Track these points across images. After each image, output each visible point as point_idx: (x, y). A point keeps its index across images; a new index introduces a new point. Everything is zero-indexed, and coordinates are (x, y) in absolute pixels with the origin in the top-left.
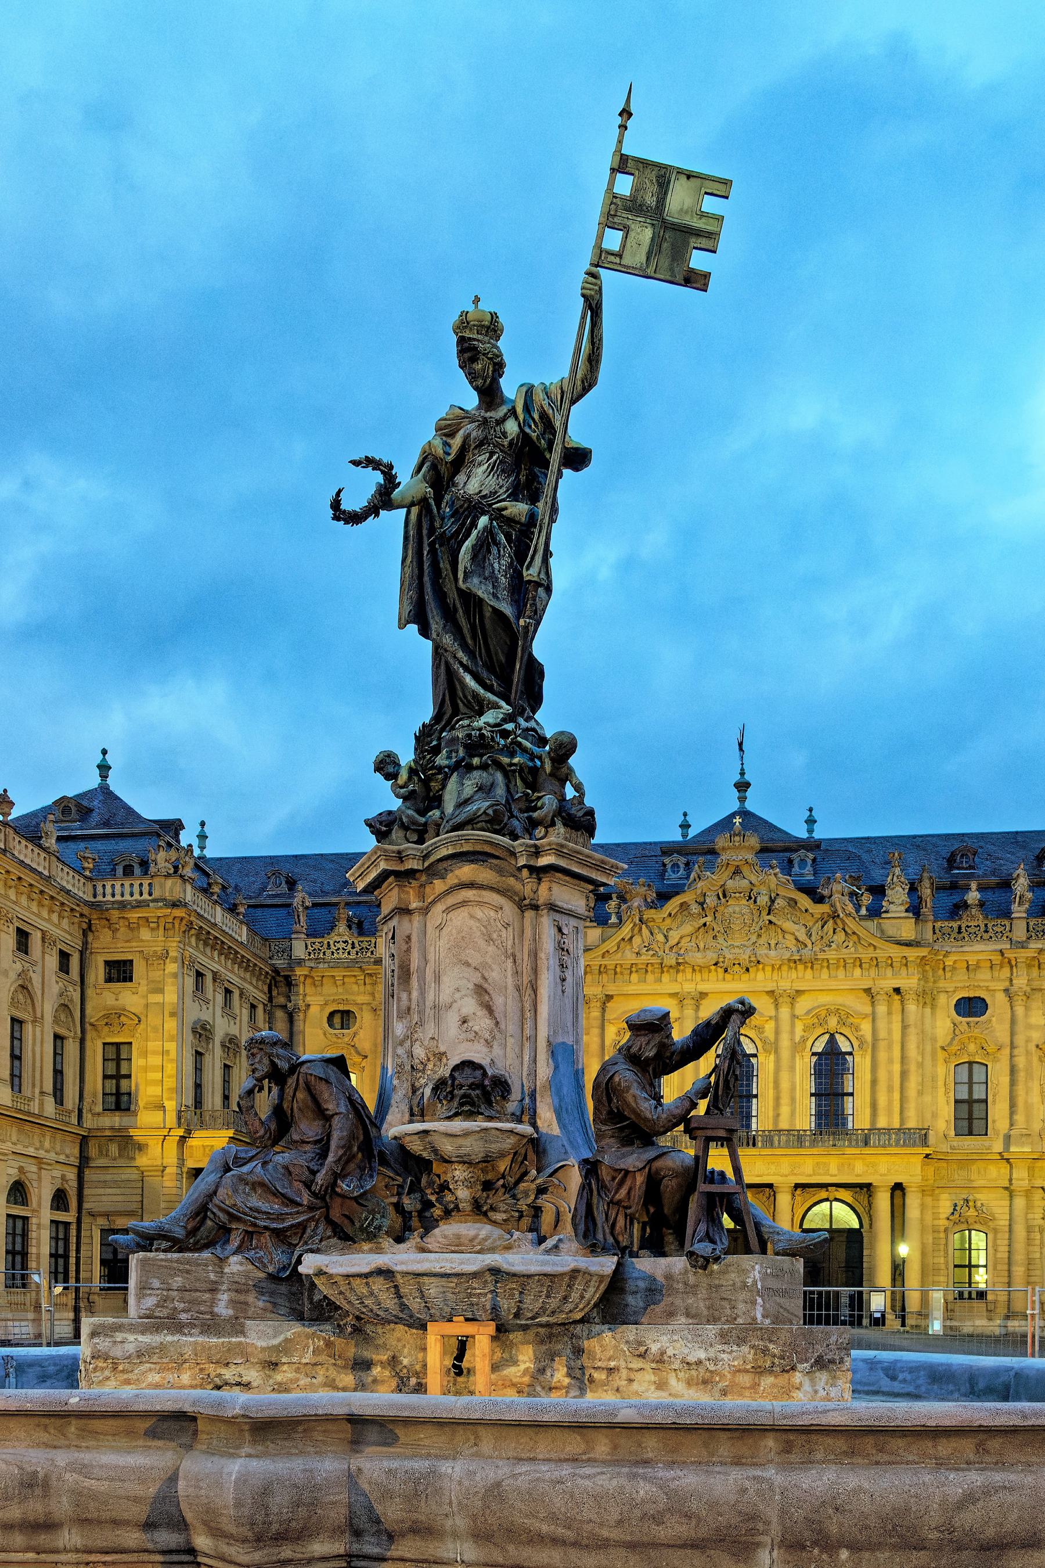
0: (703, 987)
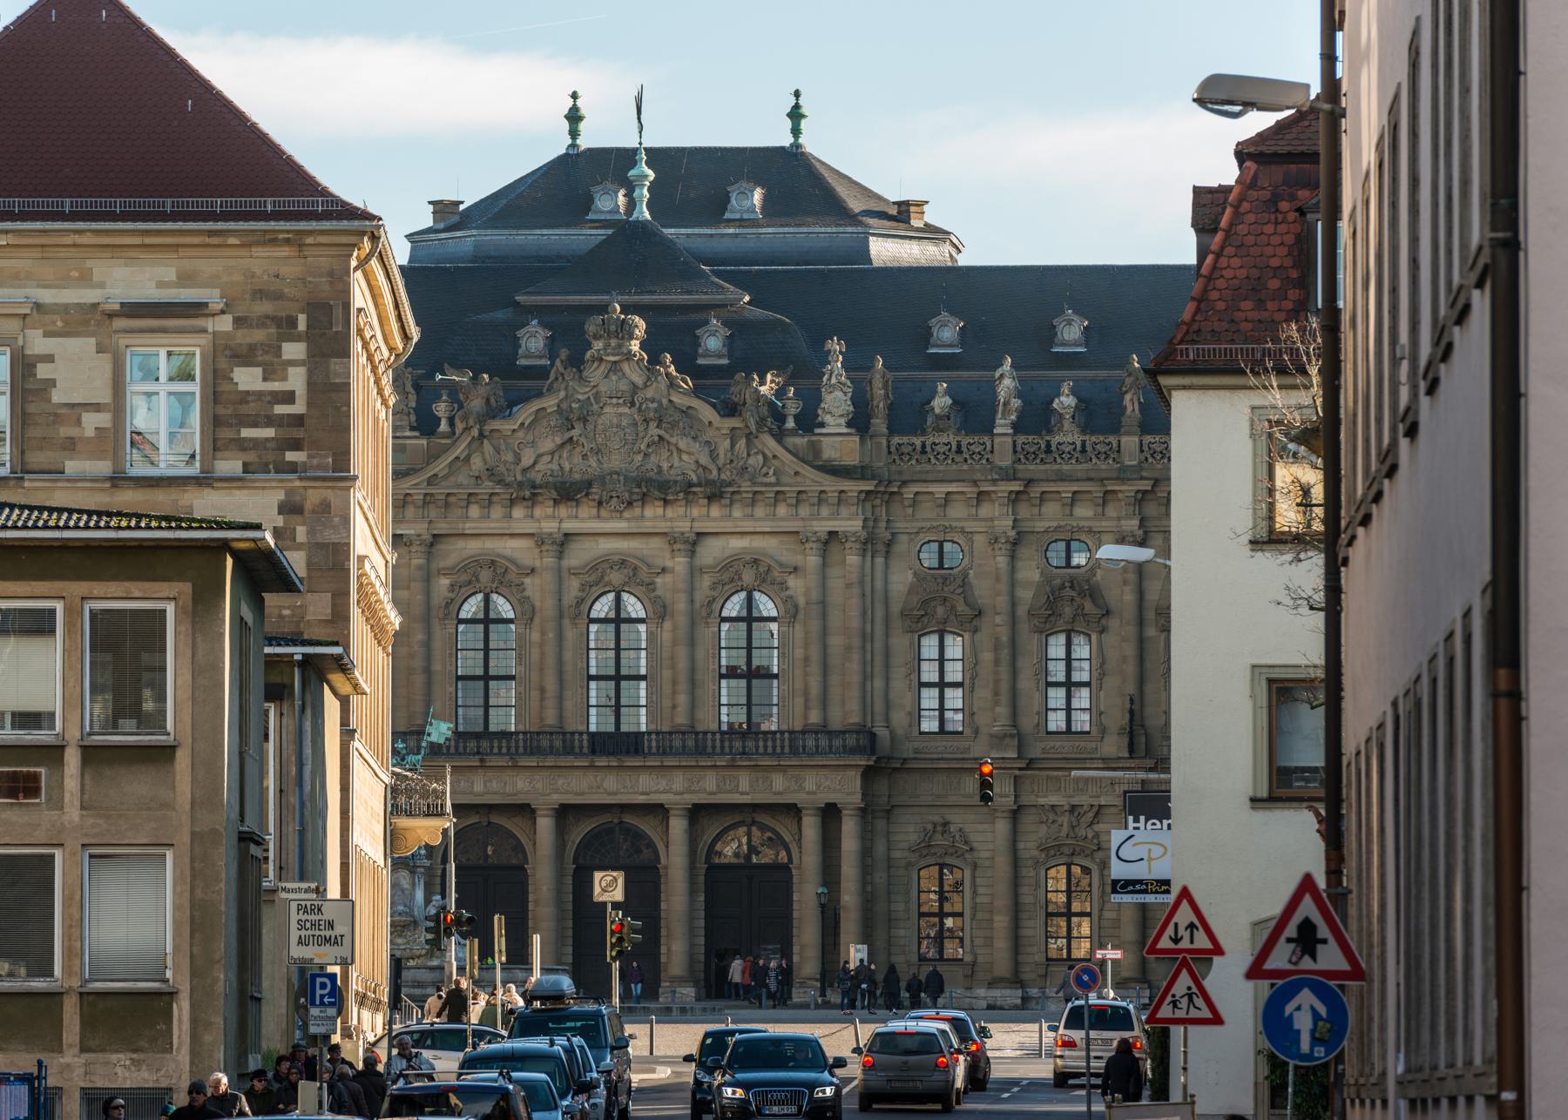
0: (569, 526)
